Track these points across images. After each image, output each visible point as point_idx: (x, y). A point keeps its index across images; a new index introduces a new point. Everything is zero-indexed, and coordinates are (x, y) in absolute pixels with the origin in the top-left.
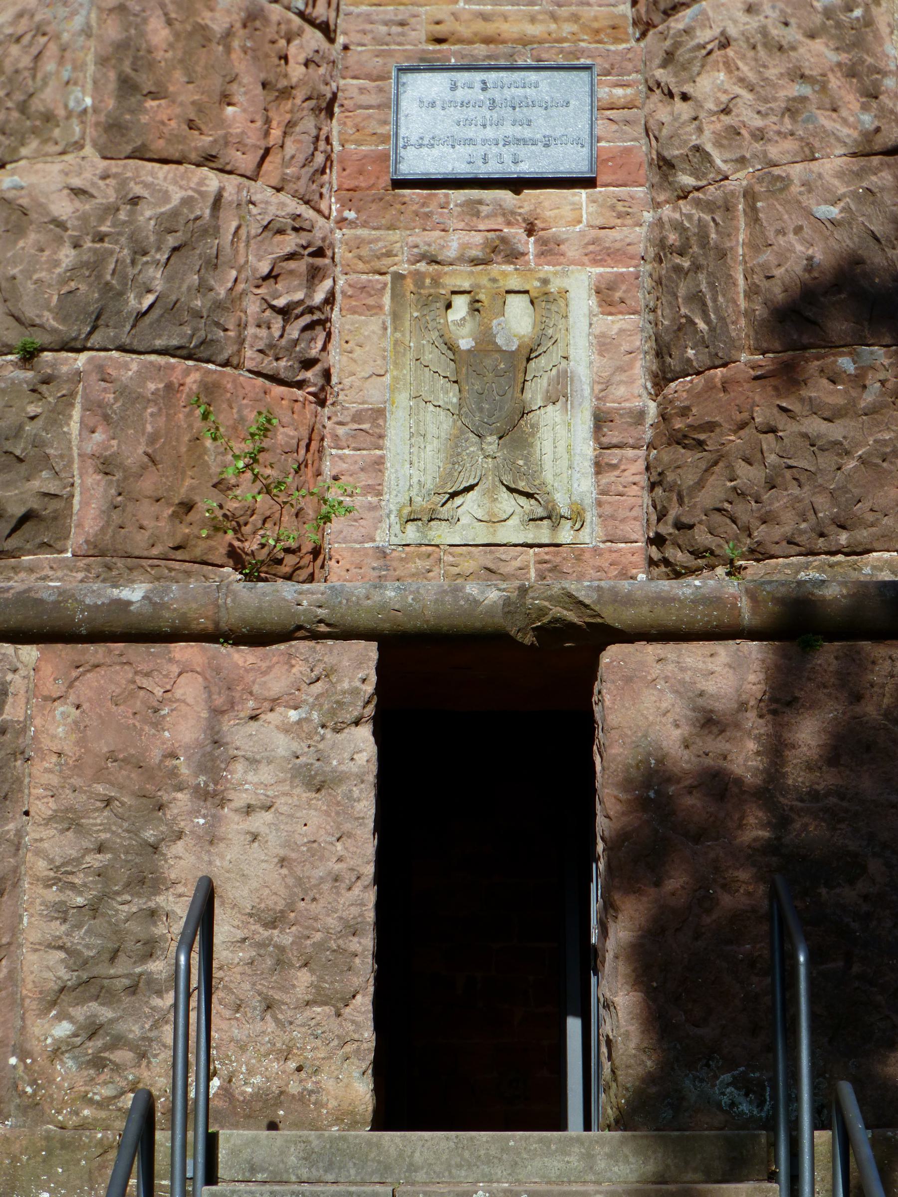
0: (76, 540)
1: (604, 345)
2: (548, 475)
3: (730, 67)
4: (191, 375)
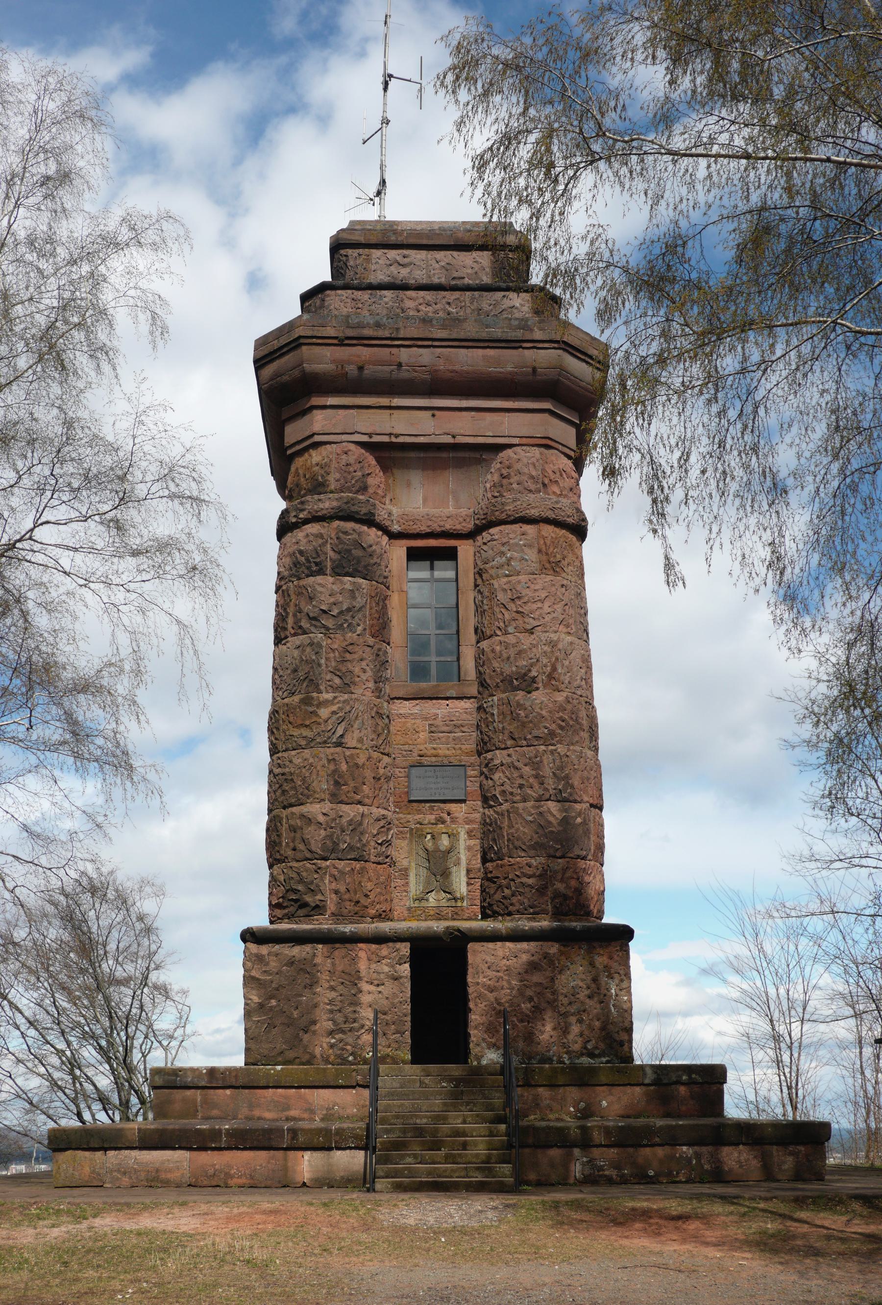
0: (329, 912)
1: (469, 848)
2: (454, 887)
3: (504, 772)
4: (358, 865)
